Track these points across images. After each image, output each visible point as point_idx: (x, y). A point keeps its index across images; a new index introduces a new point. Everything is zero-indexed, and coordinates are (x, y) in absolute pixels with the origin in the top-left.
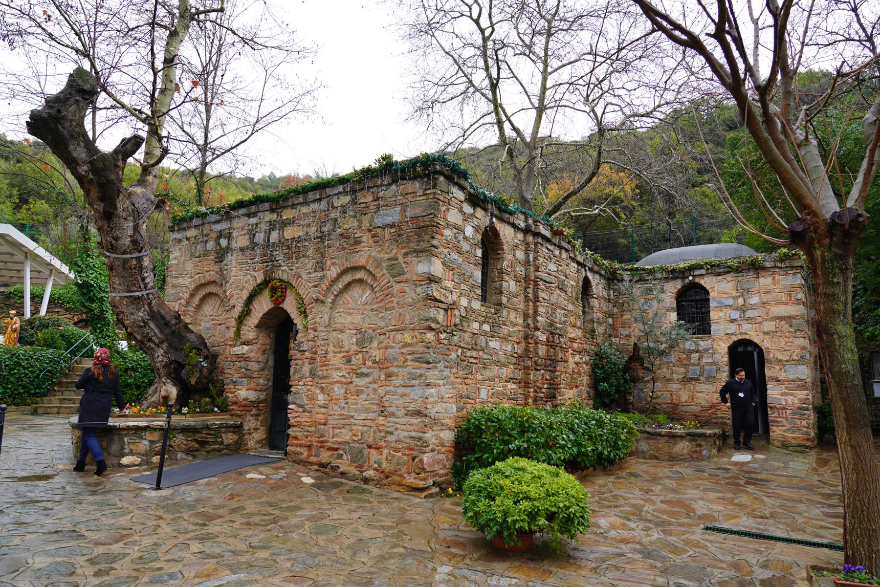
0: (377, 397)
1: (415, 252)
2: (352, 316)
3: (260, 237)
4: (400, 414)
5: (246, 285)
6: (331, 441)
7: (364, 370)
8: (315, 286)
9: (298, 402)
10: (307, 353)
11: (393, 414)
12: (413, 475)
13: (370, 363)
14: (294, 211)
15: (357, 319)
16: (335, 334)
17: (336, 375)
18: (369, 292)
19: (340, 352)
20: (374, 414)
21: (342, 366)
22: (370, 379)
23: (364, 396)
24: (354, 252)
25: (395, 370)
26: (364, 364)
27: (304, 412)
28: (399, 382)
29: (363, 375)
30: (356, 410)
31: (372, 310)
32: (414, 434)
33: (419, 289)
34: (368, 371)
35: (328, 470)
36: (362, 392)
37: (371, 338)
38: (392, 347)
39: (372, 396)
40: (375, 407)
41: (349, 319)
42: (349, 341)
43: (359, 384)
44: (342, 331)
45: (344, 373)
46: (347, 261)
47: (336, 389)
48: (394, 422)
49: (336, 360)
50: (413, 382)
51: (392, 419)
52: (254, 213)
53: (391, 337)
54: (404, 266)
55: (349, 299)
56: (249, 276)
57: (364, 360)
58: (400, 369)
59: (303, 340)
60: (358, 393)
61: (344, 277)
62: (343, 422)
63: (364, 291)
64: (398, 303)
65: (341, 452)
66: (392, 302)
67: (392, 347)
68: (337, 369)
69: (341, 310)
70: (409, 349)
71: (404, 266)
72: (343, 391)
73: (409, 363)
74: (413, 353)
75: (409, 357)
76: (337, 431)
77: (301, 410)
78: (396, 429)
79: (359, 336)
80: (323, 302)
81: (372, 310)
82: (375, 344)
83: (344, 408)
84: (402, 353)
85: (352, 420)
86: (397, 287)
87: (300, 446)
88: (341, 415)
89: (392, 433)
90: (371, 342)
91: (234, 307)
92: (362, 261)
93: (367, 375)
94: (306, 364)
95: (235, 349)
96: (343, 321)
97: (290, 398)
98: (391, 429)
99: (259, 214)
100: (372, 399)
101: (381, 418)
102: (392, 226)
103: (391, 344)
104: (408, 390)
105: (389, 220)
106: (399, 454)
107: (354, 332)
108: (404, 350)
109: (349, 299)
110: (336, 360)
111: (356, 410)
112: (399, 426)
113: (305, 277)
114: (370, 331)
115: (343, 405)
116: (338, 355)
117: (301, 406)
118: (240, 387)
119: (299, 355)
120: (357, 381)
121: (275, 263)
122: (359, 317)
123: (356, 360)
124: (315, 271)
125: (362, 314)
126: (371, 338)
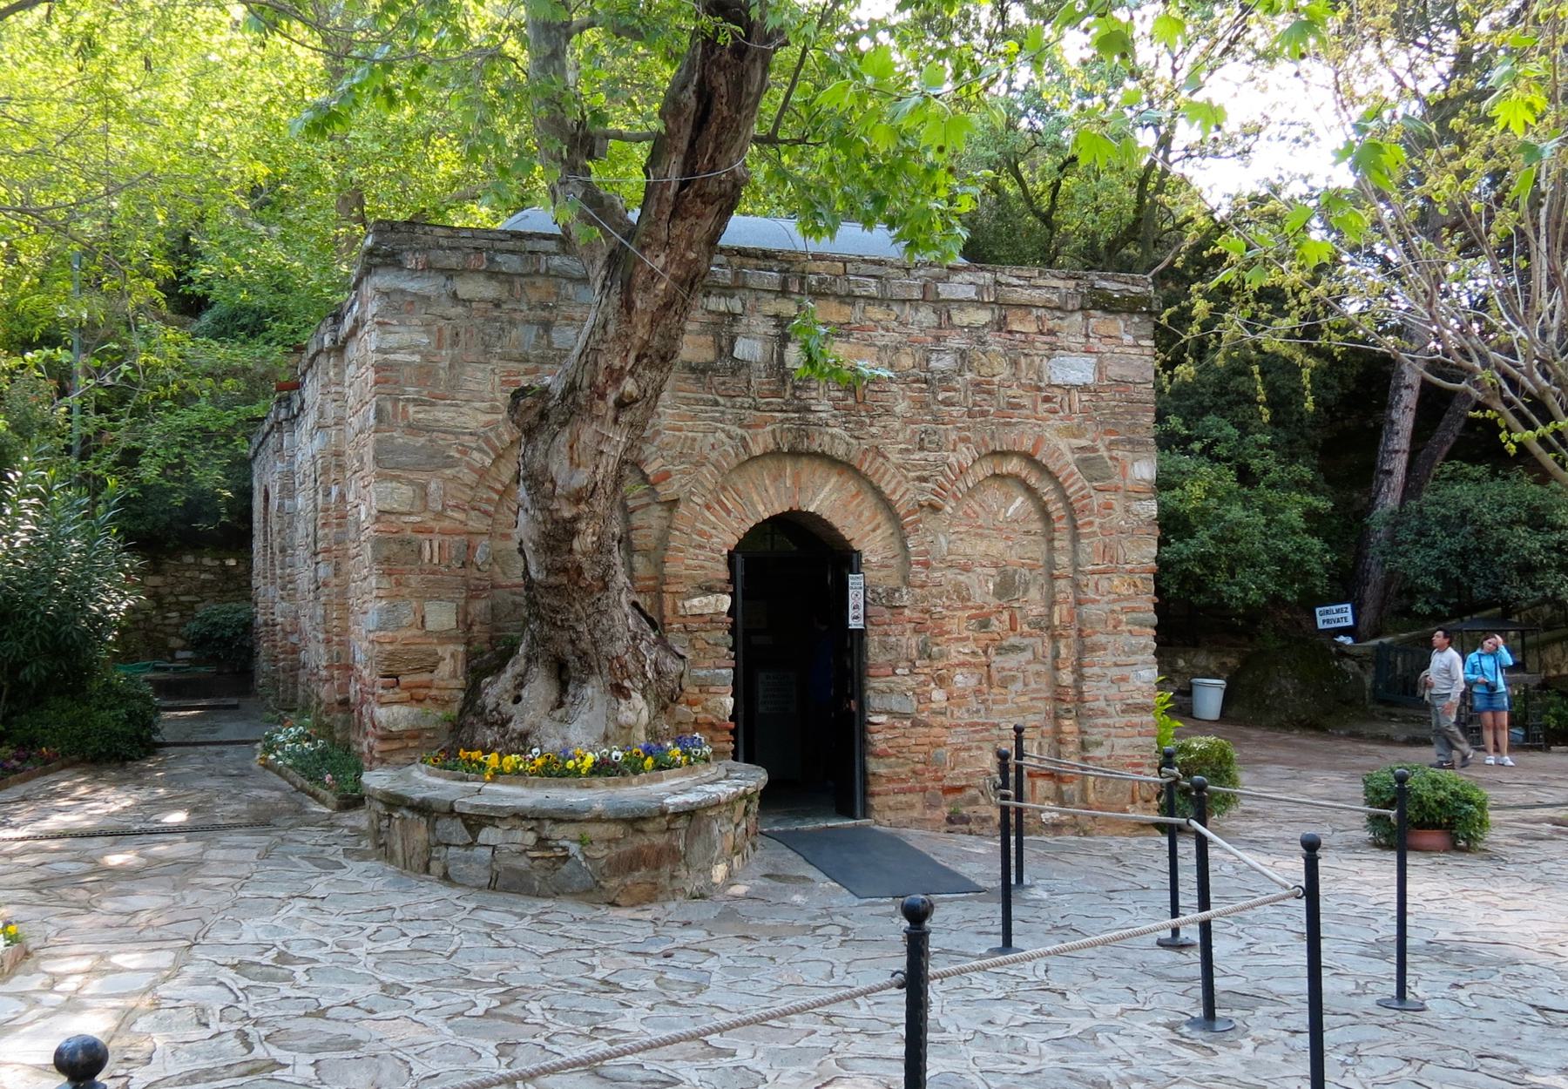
0: (1043, 686)
1: (1130, 441)
2: (985, 542)
3: (749, 348)
4: (1111, 710)
5: (714, 455)
6: (953, 777)
7: (1013, 640)
8: (925, 480)
9: (896, 708)
10: (907, 612)
11: (1104, 714)
12: (1139, 803)
13: (1026, 628)
14: (847, 309)
15: (997, 547)
16: (950, 574)
17: (957, 652)
18: (1020, 500)
19: (964, 608)
20: (1038, 717)
21: (970, 634)
22: (1028, 655)
23: (1019, 686)
24: (1009, 424)
25: (1102, 639)
26: (1013, 629)
27: (914, 725)
28: (1110, 660)
29: (1015, 648)
30: (1002, 714)
31: (1027, 533)
32: (1139, 741)
33: (1135, 506)
34: (1026, 641)
35: (973, 826)
36: (1014, 678)
37: (1027, 583)
38: (1093, 601)
39: (1033, 686)
40: (1040, 704)
41: (982, 546)
42: (982, 588)
43: (1006, 665)
44: (966, 569)
45: (971, 646)
46: (992, 438)
47: (959, 678)
48: (1104, 725)
49: (958, 623)
50: (1132, 659)
51: (1101, 721)
52: (727, 287)
53: (1091, 584)
54: (1110, 463)
55: (976, 508)
56: (723, 436)
57: (1012, 618)
58: (1112, 638)
59: (892, 583)
60: (1004, 684)
61: (977, 467)
62: (978, 736)
63: (1009, 499)
64: (1102, 526)
65: (974, 792)
66: (1091, 523)
67: (1093, 601)
68: (958, 640)
69: (962, 529)
70: (1125, 604)
71: (1110, 463)
72: (973, 682)
73: (1123, 627)
74: (1133, 610)
75: (1124, 618)
76: (964, 754)
77: (908, 723)
78: (1108, 736)
79: (998, 579)
80: (935, 509)
81: (1027, 533)
82: (1034, 594)
83: (978, 711)
84: (1113, 611)
85: (995, 732)
86: (1098, 499)
87: (911, 790)
88: (973, 725)
89: (1099, 744)
90: (1026, 591)
91: (672, 504)
92: (1027, 445)
93: (1023, 650)
94: (908, 634)
95: (695, 601)
96: (968, 551)
97: (875, 702)
98: (1098, 738)
99: (740, 293)
101: (1067, 722)
102: (1084, 388)
103: (1092, 596)
104: (1126, 671)
105: (1075, 377)
107: (993, 571)
108: (1117, 607)
109: (976, 508)
110: (958, 623)
111: (1002, 714)
112: (1113, 731)
113: (895, 458)
114: (1025, 571)
115: (975, 706)
116: (959, 613)
117: (905, 716)
118: (723, 689)
119: (887, 616)
120: (998, 661)
121: (811, 417)
122: (1001, 545)
123: (998, 625)
124: (921, 449)
125: (1008, 538)
126: (1027, 583)
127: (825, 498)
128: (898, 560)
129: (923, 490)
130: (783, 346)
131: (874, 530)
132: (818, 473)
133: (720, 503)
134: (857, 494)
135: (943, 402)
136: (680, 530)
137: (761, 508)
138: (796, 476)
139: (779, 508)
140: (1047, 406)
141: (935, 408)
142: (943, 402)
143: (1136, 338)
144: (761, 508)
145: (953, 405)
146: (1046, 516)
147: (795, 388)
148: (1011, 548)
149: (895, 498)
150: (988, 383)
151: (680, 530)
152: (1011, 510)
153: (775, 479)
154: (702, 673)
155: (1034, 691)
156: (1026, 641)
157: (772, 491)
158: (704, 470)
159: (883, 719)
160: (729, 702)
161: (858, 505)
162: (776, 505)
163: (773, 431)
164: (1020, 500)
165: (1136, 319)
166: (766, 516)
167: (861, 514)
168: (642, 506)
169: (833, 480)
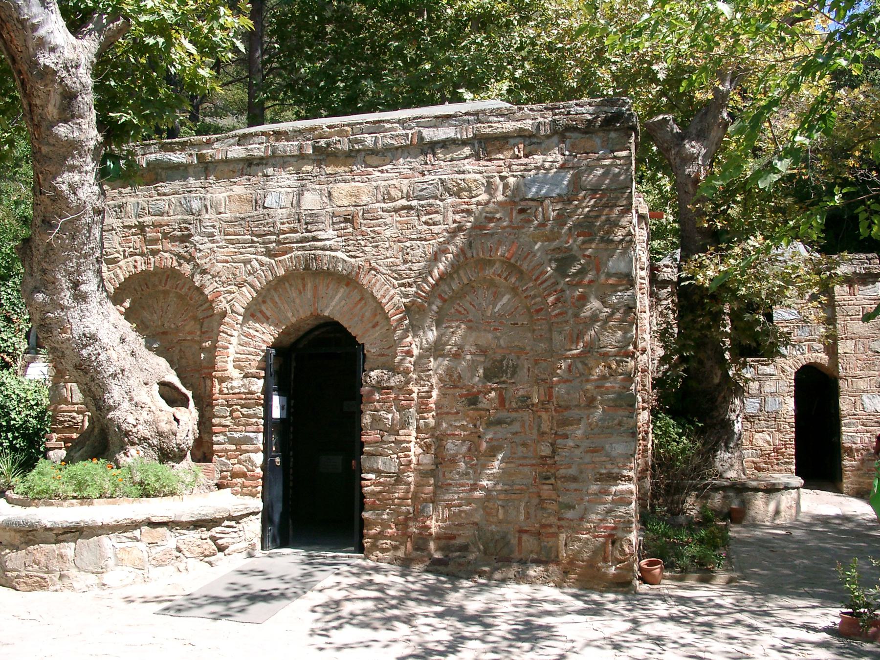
7: (503, 414)
19: (455, 387)
22: (516, 427)
55: (467, 305)
63: (497, 296)
83: (467, 474)
100: (525, 458)
109: (467, 305)
125: (496, 329)
127: (336, 305)
129: (406, 296)
130: (300, 195)
131: (374, 327)
132: (331, 286)
133: (261, 312)
134: (361, 300)
135: (426, 223)
136: (226, 333)
137: (290, 315)
138: (315, 288)
139: (304, 312)
140: (522, 216)
141: (419, 228)
142: (426, 223)
144: (290, 315)
145: (434, 224)
147: (307, 224)
148: (498, 338)
149: (384, 301)
150: (467, 203)
151: (226, 333)
152: (498, 307)
153: (301, 293)
154: (236, 435)
155: (519, 458)
157: (298, 301)
158: (244, 289)
159: (372, 476)
160: (258, 458)
161: (361, 308)
162: (301, 312)
163: (291, 257)
165: (613, 135)
166: (294, 320)
167: (363, 317)
168: (207, 317)
169: (342, 290)
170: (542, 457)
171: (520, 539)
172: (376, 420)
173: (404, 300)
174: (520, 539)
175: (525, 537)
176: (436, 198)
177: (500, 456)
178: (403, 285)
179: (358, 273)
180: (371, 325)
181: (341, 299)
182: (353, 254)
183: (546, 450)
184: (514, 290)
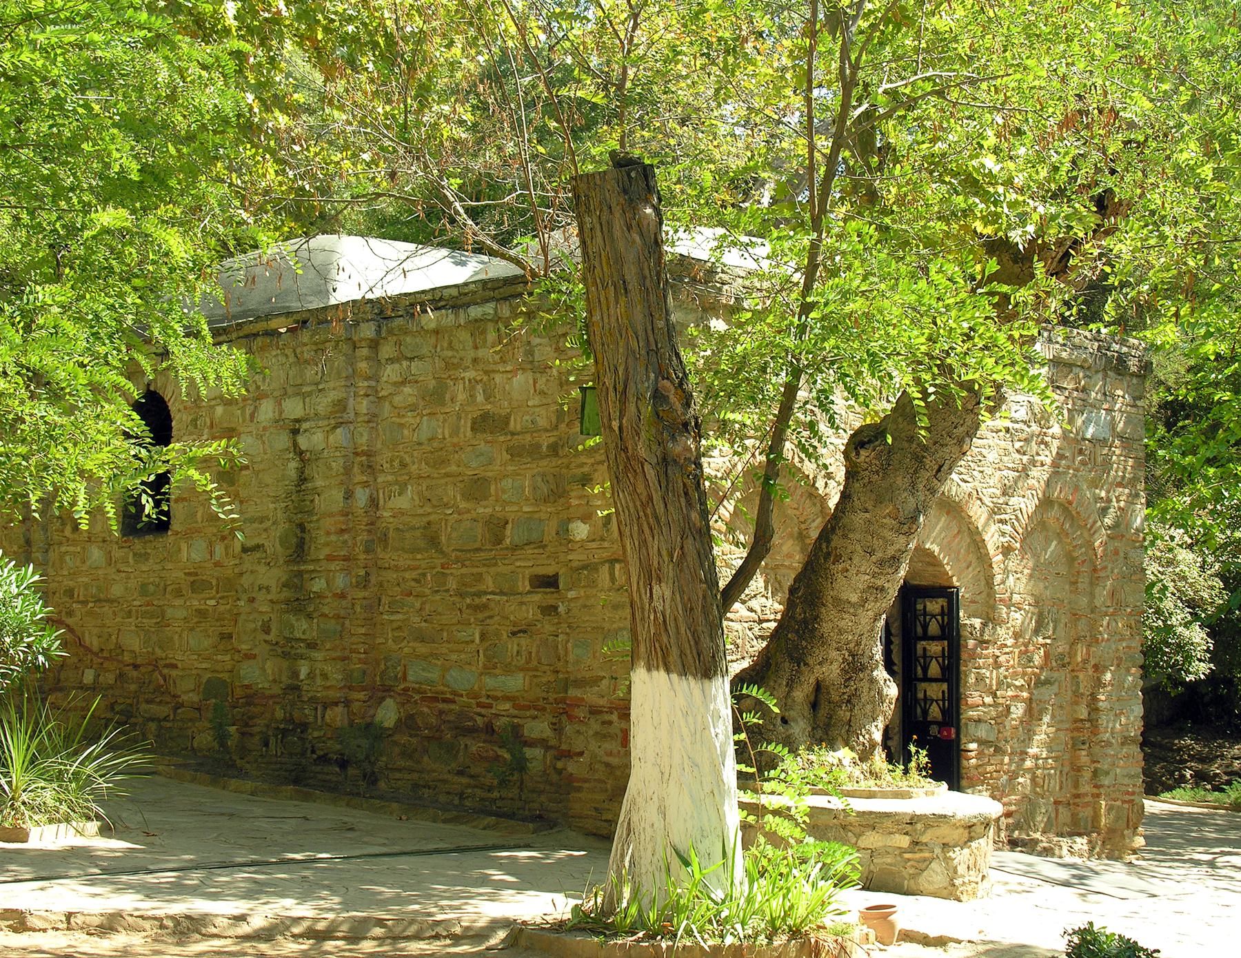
22: (1055, 688)
29: (1047, 682)
63: (1048, 541)
83: (1023, 741)
89: (1107, 773)
106: (1119, 803)
128: (984, 595)
129: (1003, 534)
143: (1135, 399)
146: (1071, 560)
156: (1056, 675)
164: (1054, 543)
170: (1077, 721)
171: (1057, 811)
172: (980, 679)
173: (1002, 539)
174: (1057, 811)
175: (1060, 808)
176: (1025, 422)
177: (1047, 719)
178: (1001, 521)
179: (967, 502)
180: (964, 565)
181: (942, 530)
182: (965, 477)
183: (1083, 713)
184: (1061, 535)
